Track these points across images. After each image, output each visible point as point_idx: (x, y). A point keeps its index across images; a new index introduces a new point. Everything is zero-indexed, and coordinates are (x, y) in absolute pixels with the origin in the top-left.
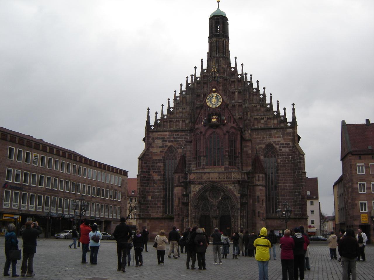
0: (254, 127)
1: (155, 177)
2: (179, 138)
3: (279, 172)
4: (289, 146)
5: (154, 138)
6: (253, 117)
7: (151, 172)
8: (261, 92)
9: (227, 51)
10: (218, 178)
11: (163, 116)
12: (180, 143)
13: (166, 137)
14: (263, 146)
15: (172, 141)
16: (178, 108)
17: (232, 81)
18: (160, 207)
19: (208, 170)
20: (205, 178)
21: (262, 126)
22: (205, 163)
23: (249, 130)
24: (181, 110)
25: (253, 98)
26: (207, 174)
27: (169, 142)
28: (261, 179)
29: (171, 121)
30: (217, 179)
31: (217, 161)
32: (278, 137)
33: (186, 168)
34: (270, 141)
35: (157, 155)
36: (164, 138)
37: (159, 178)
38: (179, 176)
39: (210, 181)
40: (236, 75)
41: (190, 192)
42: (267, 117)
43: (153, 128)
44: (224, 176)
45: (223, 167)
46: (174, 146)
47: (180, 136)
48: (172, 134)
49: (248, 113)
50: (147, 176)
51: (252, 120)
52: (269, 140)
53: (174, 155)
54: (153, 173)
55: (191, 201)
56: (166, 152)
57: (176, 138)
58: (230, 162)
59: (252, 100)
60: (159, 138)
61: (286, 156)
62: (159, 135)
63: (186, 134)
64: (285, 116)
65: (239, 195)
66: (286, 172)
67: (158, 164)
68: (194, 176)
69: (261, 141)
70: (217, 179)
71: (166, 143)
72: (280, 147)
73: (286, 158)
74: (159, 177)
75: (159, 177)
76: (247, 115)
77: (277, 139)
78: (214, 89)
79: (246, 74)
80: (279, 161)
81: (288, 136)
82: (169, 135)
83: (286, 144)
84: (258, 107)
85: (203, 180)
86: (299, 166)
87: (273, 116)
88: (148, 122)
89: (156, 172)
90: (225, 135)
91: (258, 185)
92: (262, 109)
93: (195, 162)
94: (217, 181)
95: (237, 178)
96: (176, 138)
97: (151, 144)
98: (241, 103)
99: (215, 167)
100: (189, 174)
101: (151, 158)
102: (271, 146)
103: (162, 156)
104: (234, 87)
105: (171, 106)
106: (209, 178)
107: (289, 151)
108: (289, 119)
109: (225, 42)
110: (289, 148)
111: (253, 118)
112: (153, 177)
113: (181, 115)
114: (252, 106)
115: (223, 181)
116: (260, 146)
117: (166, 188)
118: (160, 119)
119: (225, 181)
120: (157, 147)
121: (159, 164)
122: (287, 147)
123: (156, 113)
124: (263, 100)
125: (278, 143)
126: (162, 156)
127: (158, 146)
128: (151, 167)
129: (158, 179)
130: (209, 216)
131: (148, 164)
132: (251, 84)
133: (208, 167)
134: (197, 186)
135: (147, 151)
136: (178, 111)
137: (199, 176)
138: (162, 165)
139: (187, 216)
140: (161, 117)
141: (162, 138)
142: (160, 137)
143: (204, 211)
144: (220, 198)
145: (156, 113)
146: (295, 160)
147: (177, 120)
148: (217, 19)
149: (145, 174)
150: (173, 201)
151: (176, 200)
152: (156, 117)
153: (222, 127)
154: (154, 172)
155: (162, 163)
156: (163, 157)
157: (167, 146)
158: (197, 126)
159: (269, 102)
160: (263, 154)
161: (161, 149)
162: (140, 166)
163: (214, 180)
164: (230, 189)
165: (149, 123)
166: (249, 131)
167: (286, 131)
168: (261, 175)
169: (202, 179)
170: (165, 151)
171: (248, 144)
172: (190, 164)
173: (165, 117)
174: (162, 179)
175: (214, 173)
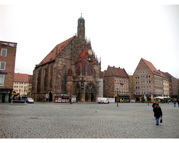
7: (58, 74)
18: (61, 89)
20: (89, 80)
24: (68, 51)
27: (64, 63)
29: (65, 55)
37: (60, 77)
39: (90, 81)
41: (84, 85)
64: (98, 61)
77: (96, 68)
89: (59, 74)
90: (93, 65)
96: (67, 62)
101: (58, 68)
108: (99, 62)
113: (68, 53)
117: (62, 81)
136: (67, 51)
141: (62, 61)
142: (61, 60)
144: (92, 87)
153: (92, 62)
154: (58, 74)
158: (83, 60)
161: (61, 65)
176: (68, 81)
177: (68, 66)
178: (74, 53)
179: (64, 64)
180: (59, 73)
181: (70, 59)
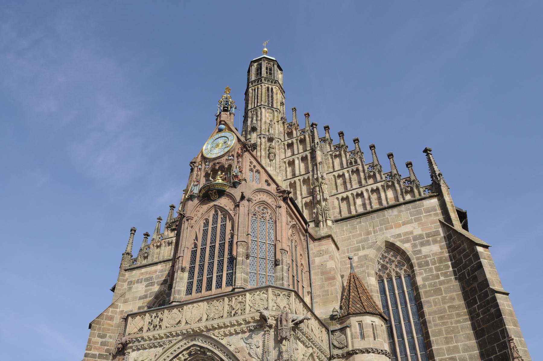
0: (341, 216)
3: (426, 309)
4: (439, 239)
6: (337, 196)
13: (154, 276)
14: (371, 253)
32: (404, 224)
36: (151, 278)
52: (383, 236)
60: (142, 279)
61: (437, 265)
62: (142, 274)
66: (446, 306)
69: (360, 242)
70: (200, 320)
72: (414, 246)
73: (438, 269)
78: (222, 126)
80: (419, 280)
81: (430, 215)
83: (428, 235)
86: (480, 280)
87: (383, 183)
107: (441, 249)
109: (272, 89)
110: (440, 242)
114: (334, 175)
116: (361, 253)
120: (134, 299)
122: (435, 242)
125: (408, 238)
127: (136, 297)
135: (111, 309)
141: (147, 280)
146: (465, 267)
160: (373, 272)
166: (329, 223)
167: (423, 206)
168: (368, 319)
171: (323, 248)
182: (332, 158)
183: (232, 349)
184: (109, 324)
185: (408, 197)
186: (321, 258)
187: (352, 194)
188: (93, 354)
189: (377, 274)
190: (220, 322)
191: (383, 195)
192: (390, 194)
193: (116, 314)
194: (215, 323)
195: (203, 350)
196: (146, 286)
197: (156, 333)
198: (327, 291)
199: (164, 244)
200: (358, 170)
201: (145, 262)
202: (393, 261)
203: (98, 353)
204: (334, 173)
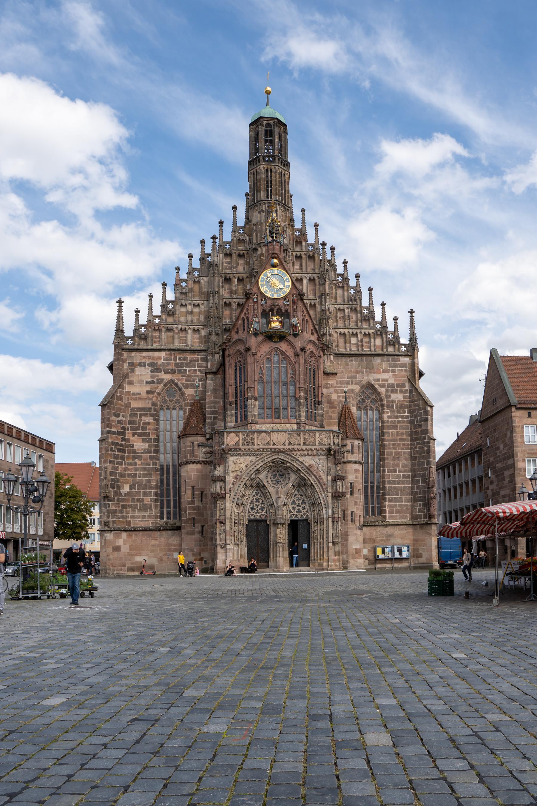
1: (137, 444)
2: (187, 365)
5: (133, 363)
6: (337, 330)
7: (129, 435)
8: (353, 283)
9: (287, 194)
10: (287, 444)
11: (151, 319)
12: (189, 376)
13: (159, 363)
14: (357, 388)
15: (173, 372)
16: (184, 304)
17: (296, 257)
19: (264, 427)
20: (259, 441)
21: (354, 348)
22: (257, 414)
23: (330, 355)
24: (190, 307)
25: (336, 293)
26: (263, 434)
27: (167, 372)
28: (356, 449)
29: (169, 330)
30: (284, 444)
31: (281, 410)
33: (207, 427)
34: (370, 379)
35: (141, 399)
37: (146, 446)
38: (193, 443)
40: (304, 244)
42: (363, 331)
43: (130, 342)
44: (298, 438)
45: (295, 421)
46: (176, 381)
47: (190, 360)
48: (173, 356)
49: (329, 321)
50: (120, 442)
51: (335, 336)
53: (177, 400)
54: (133, 436)
55: (230, 491)
56: (159, 394)
57: (182, 365)
58: (307, 412)
59: (336, 298)
62: (144, 357)
63: (201, 358)
65: (330, 478)
67: (143, 418)
68: (237, 439)
69: (350, 378)
71: (160, 374)
74: (147, 445)
75: (147, 445)
76: (327, 324)
79: (324, 244)
82: (166, 359)
84: (346, 311)
85: (256, 447)
87: (374, 331)
88: (119, 331)
89: (140, 435)
91: (352, 462)
92: (353, 316)
93: (234, 412)
94: (284, 449)
95: (326, 444)
97: (126, 376)
98: (315, 301)
99: (276, 421)
100: (225, 434)
102: (370, 389)
103: (151, 401)
104: (301, 269)
105: (168, 299)
106: (268, 444)
109: (284, 175)
111: (336, 332)
112: (133, 445)
113: (190, 318)
114: (335, 308)
115: (298, 450)
116: (350, 387)
118: (146, 323)
119: (302, 450)
120: (141, 382)
121: (146, 419)
123: (137, 311)
124: (357, 298)
126: (151, 401)
128: (129, 424)
129: (145, 450)
130: (266, 521)
131: (121, 418)
132: (333, 266)
133: (263, 420)
134: (242, 459)
135: (119, 390)
136: (183, 310)
137: (249, 439)
138: (152, 421)
139: (223, 523)
140: (149, 321)
143: (255, 511)
145: (137, 311)
147: (183, 327)
148: (268, 125)
149: (117, 437)
150: (178, 493)
151: (187, 491)
152: (137, 319)
154: (134, 434)
155: (151, 415)
156: (154, 404)
157: (163, 380)
159: (367, 304)
160: (355, 403)
161: (148, 388)
162: (106, 420)
163: (279, 447)
164: (311, 466)
165: (122, 331)
168: (357, 443)
169: (254, 445)
170: (157, 391)
171: (330, 382)
172: (215, 418)
173: (157, 321)
174: (153, 449)
175: (279, 433)
176: (187, 463)
177: (193, 386)
178: (227, 312)
179: (167, 377)
180: (138, 429)
181: (202, 347)
182: (335, 288)
183: (307, 464)
184: (120, 404)
185: (391, 349)
186: (328, 389)
187: (349, 332)
188: (113, 432)
189: (357, 404)
190: (299, 447)
191: (372, 340)
192: (378, 342)
193: (123, 394)
194: (296, 447)
195: (283, 462)
196: (151, 371)
197: (251, 447)
198: (331, 416)
199: (163, 330)
200: (356, 309)
201: (142, 345)
202: (370, 398)
203: (116, 431)
204: (336, 306)
